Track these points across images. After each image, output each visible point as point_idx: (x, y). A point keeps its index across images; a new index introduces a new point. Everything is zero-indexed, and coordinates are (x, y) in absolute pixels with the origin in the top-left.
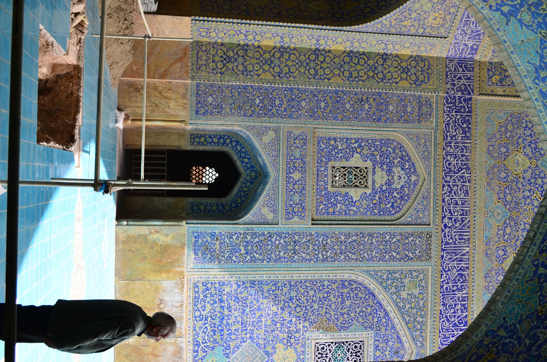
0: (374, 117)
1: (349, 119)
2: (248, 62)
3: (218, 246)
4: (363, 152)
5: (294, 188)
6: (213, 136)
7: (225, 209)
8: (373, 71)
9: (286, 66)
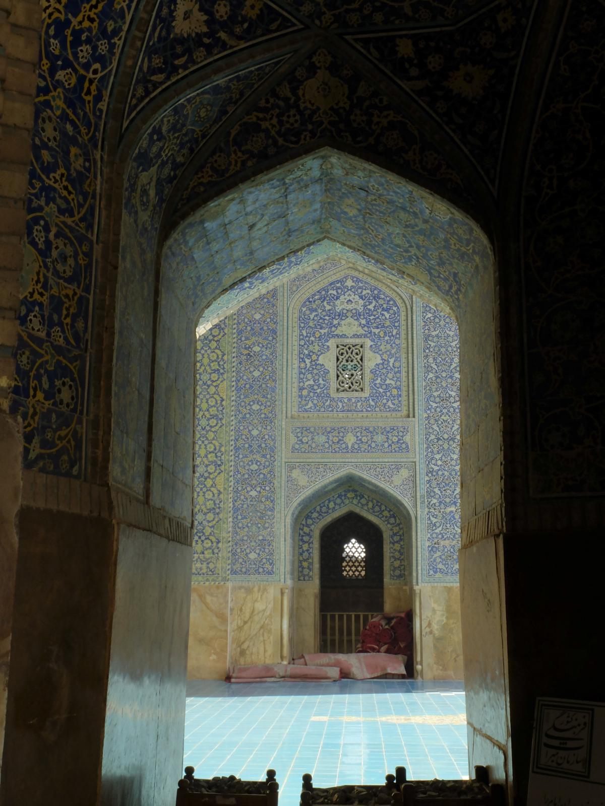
0: (270, 338)
1: (274, 372)
2: (203, 507)
3: (447, 542)
4: (316, 351)
5: (367, 443)
7: (398, 532)
8: (210, 341)
9: (206, 456)
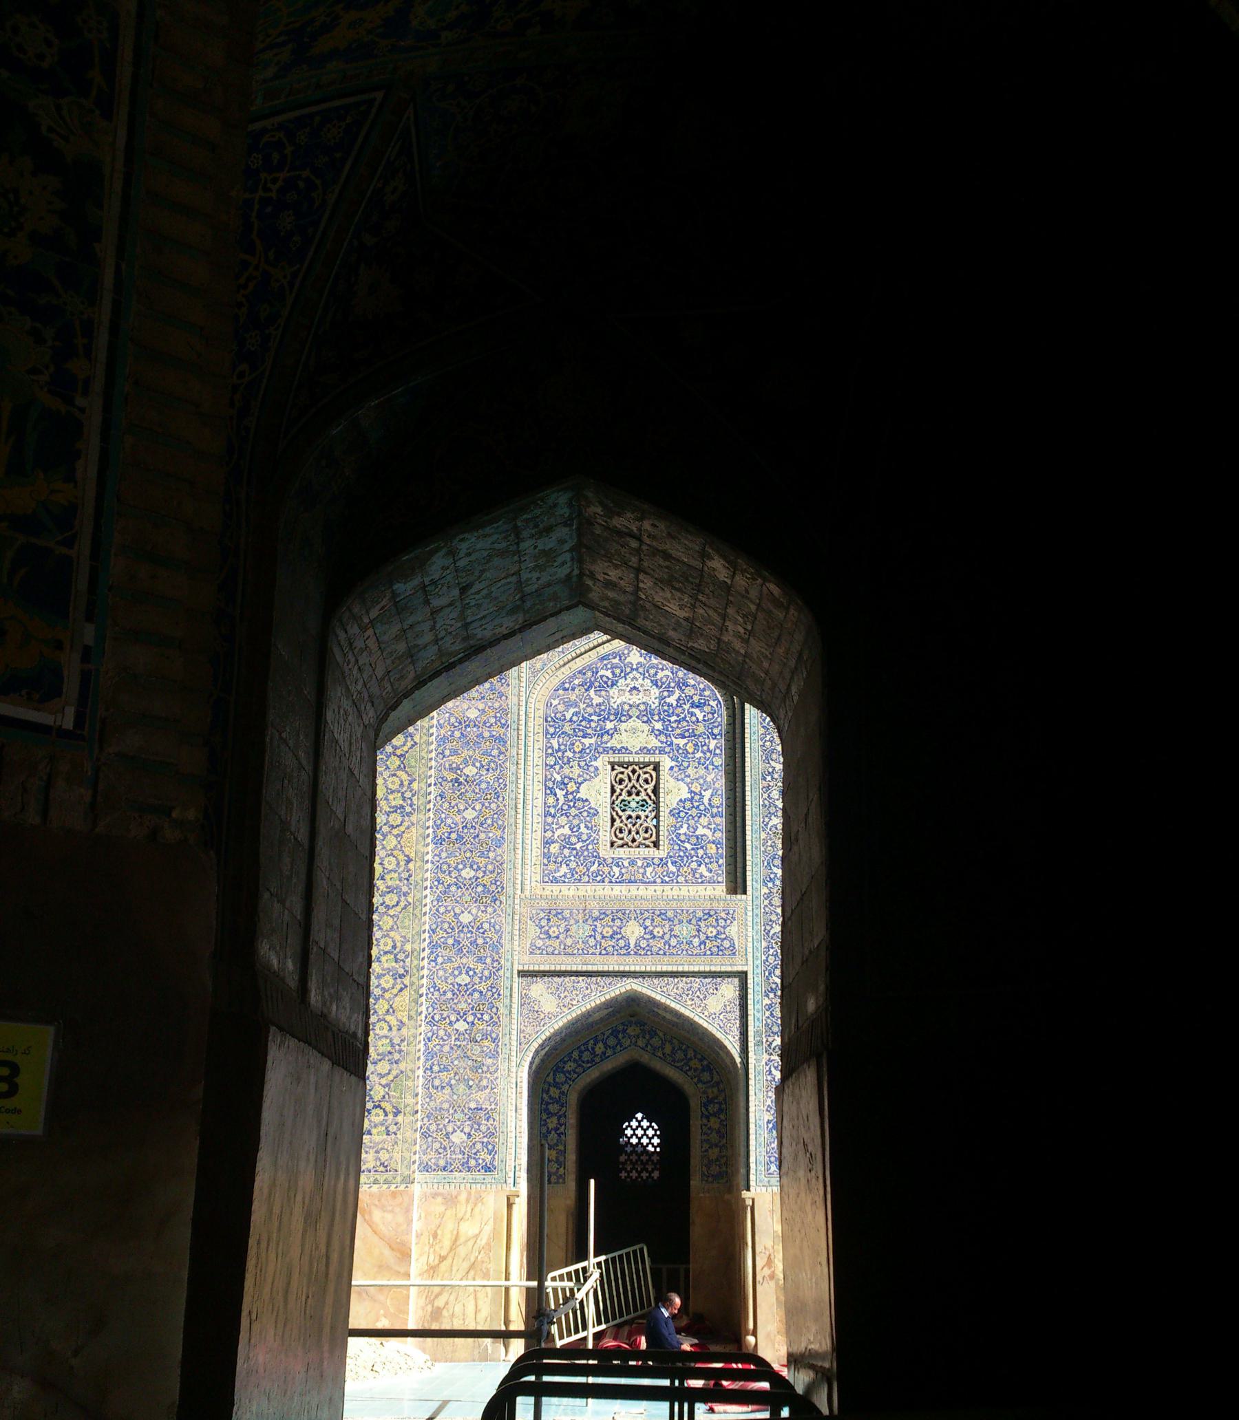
0: (495, 752)
1: (500, 813)
5: (662, 938)
6: (544, 1130)
7: (716, 1098)
